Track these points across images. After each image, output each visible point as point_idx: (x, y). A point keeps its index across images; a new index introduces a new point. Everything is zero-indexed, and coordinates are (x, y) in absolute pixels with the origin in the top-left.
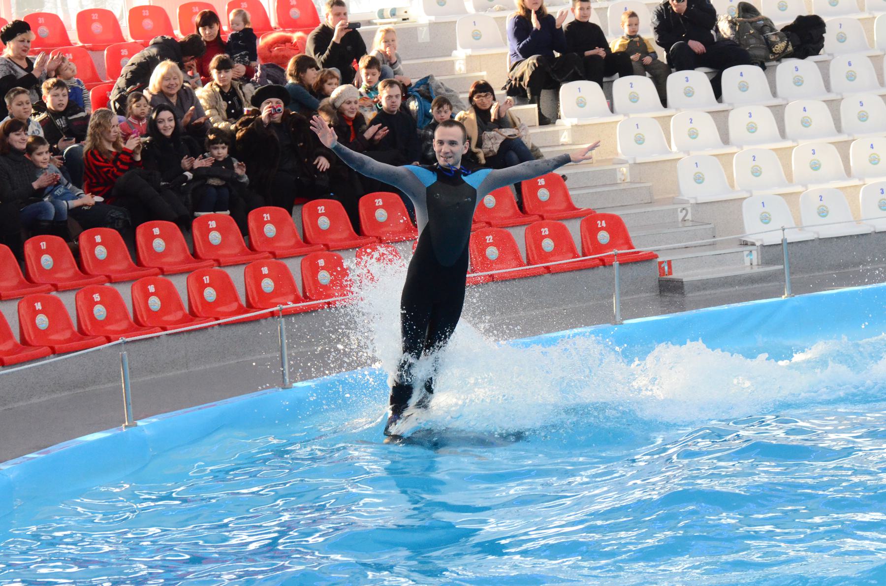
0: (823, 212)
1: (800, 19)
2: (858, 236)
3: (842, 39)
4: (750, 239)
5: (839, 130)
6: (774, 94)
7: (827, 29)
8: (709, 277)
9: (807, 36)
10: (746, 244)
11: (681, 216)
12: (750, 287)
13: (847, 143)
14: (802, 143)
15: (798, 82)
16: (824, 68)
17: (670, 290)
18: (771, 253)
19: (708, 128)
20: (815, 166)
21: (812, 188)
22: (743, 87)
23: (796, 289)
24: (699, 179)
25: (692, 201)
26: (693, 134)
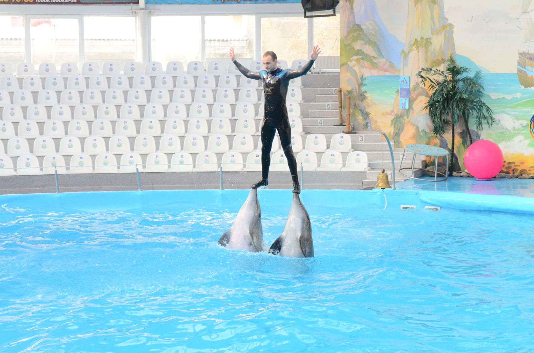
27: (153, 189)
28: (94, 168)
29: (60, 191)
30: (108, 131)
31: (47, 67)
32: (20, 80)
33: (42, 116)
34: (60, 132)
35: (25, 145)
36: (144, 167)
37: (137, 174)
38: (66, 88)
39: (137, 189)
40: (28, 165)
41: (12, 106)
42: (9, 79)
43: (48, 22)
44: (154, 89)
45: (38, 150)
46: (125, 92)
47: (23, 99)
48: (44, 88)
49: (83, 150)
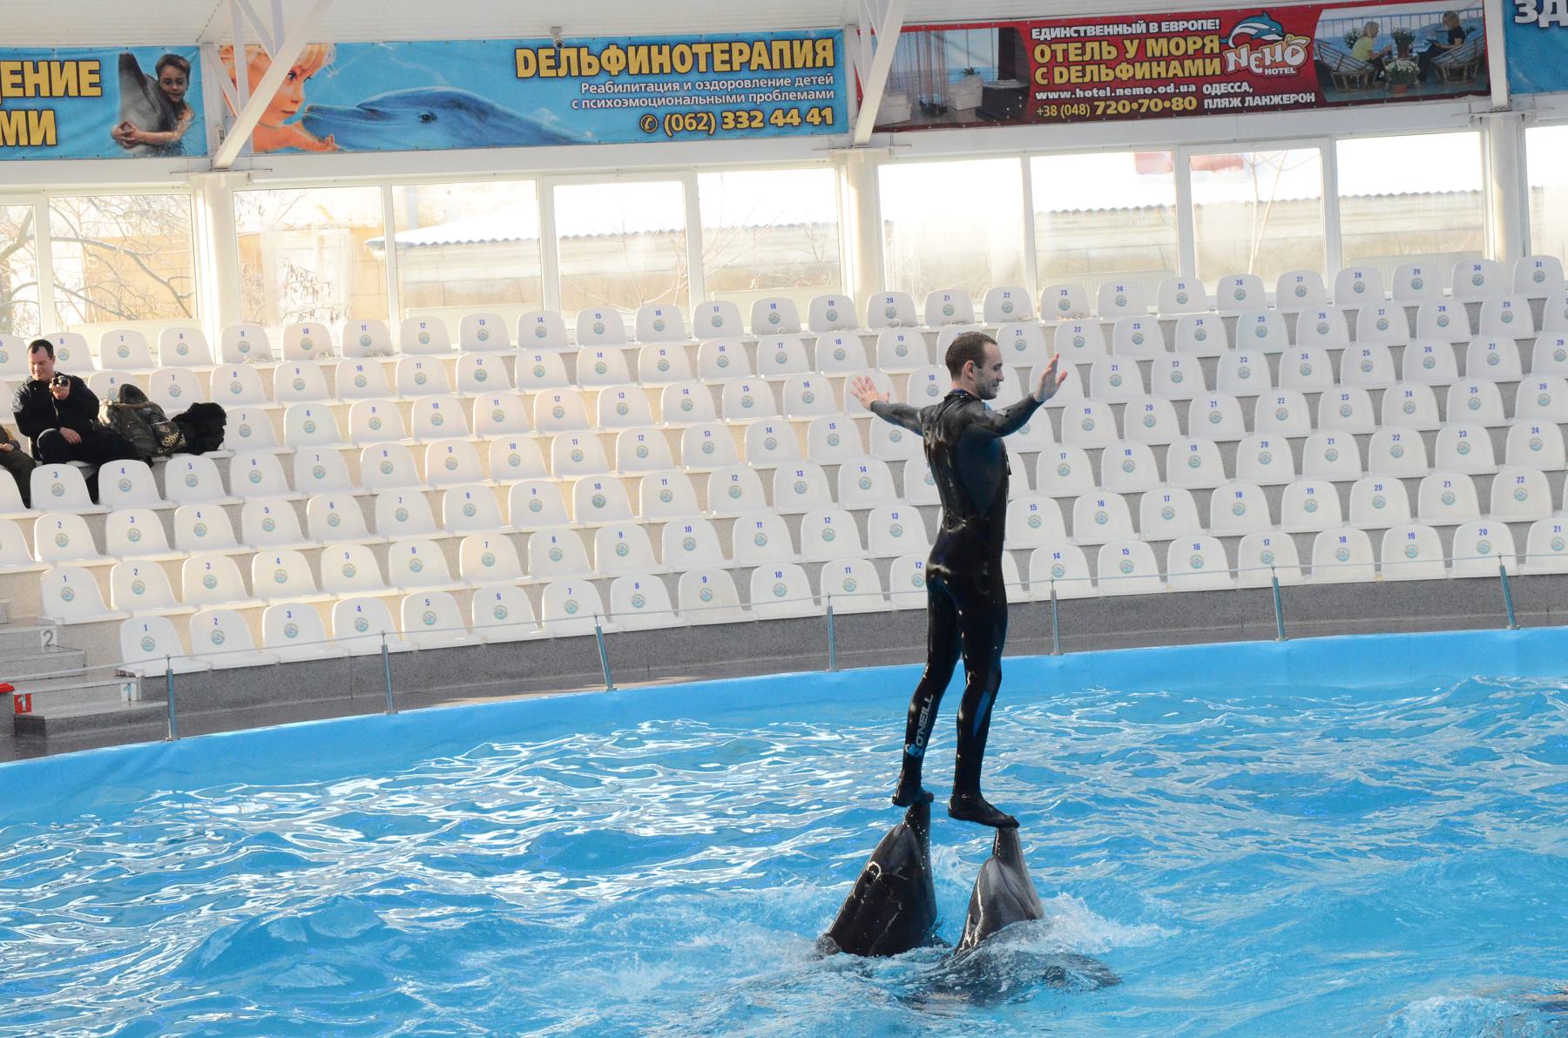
0: (218, 639)
1: (196, 407)
2: (259, 667)
3: (245, 432)
4: (129, 669)
5: (240, 540)
6: (163, 496)
7: (228, 420)
8: (78, 714)
9: (203, 428)
10: (123, 675)
11: (44, 640)
12: (128, 727)
13: (250, 556)
14: (195, 555)
15: (192, 482)
16: (223, 466)
17: (29, 732)
18: (157, 686)
19: (80, 534)
20: (210, 583)
21: (205, 609)
22: (125, 487)
23: (181, 732)
24: (67, 596)
25: (59, 623)
26: (62, 541)
27: (1549, 623)
28: (1378, 568)
29: (1286, 635)
30: (1414, 461)
31: (1238, 288)
32: (1168, 326)
33: (1232, 425)
34: (1280, 468)
35: (1187, 508)
36: (1521, 560)
37: (1504, 579)
38: (1292, 342)
39: (1502, 624)
40: (1197, 563)
41: (1148, 400)
42: (1137, 326)
43: (1240, 164)
44: (1540, 336)
45: (1224, 522)
46: (1460, 348)
47: (1177, 378)
48: (1232, 345)
49: (1345, 517)
